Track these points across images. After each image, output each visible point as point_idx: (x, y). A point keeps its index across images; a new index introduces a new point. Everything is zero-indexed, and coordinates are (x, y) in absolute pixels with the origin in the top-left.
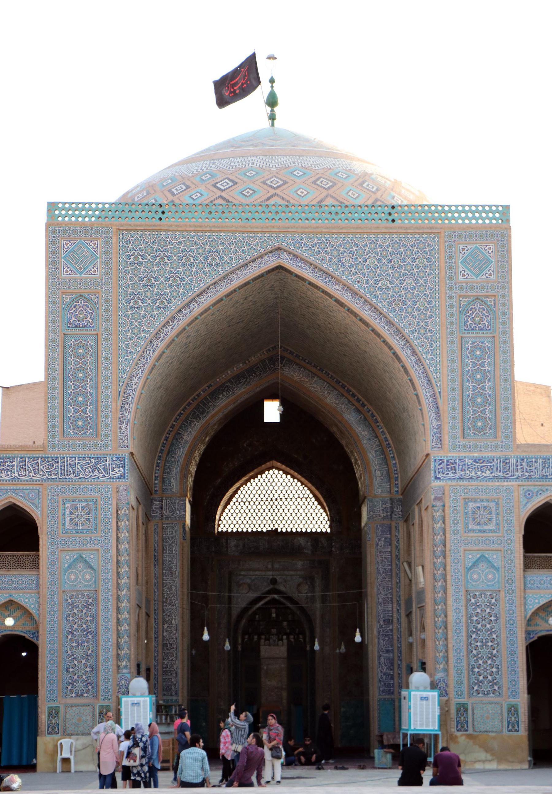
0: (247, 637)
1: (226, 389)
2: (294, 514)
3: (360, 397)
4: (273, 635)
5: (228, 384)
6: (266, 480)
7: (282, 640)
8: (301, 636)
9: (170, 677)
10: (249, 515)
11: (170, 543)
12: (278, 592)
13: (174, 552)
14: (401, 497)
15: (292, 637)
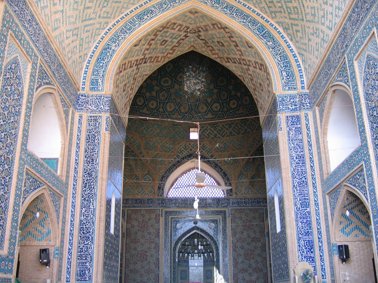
0: (181, 254)
1: (151, 12)
2: (206, 192)
3: (264, 16)
4: (195, 253)
5: (153, 9)
6: (192, 175)
7: (200, 256)
8: (211, 254)
9: (84, 261)
10: (183, 192)
11: (94, 133)
12: (198, 228)
13: (96, 141)
14: (308, 91)
15: (206, 254)
